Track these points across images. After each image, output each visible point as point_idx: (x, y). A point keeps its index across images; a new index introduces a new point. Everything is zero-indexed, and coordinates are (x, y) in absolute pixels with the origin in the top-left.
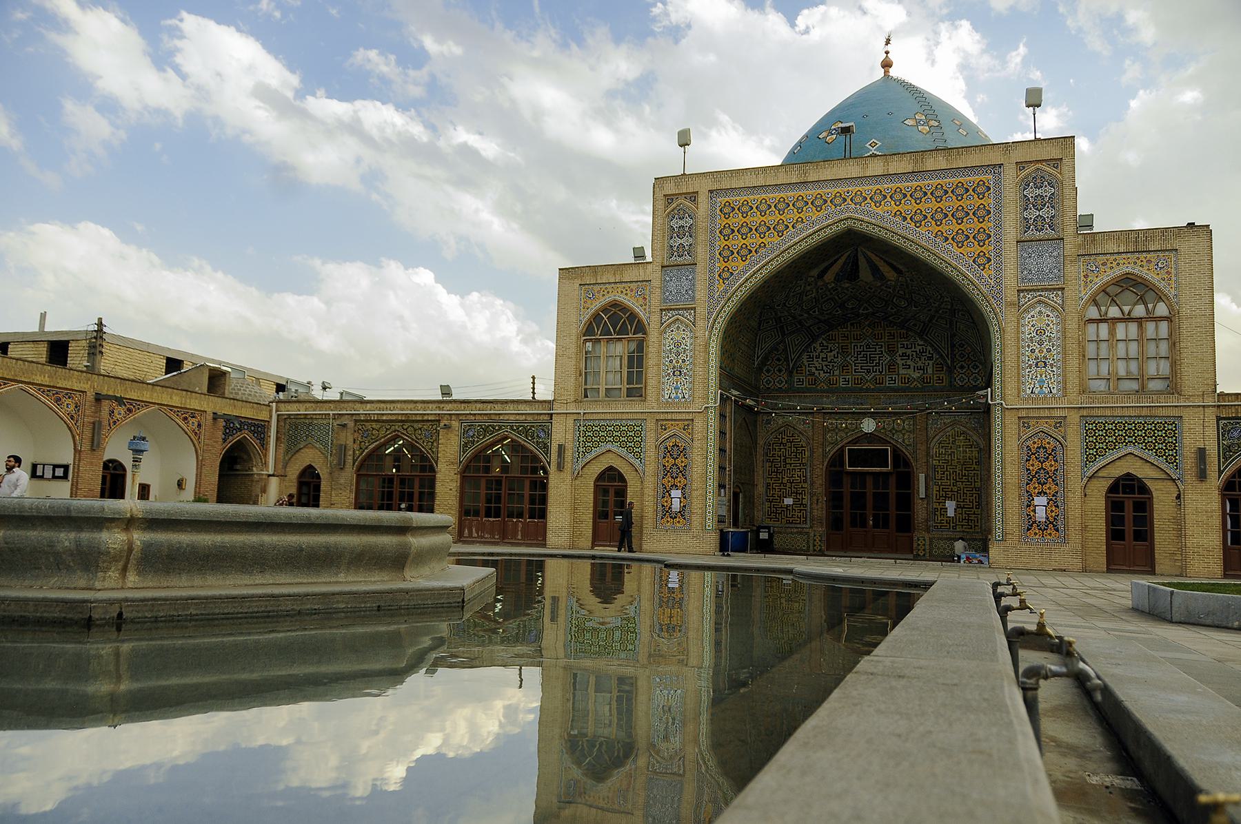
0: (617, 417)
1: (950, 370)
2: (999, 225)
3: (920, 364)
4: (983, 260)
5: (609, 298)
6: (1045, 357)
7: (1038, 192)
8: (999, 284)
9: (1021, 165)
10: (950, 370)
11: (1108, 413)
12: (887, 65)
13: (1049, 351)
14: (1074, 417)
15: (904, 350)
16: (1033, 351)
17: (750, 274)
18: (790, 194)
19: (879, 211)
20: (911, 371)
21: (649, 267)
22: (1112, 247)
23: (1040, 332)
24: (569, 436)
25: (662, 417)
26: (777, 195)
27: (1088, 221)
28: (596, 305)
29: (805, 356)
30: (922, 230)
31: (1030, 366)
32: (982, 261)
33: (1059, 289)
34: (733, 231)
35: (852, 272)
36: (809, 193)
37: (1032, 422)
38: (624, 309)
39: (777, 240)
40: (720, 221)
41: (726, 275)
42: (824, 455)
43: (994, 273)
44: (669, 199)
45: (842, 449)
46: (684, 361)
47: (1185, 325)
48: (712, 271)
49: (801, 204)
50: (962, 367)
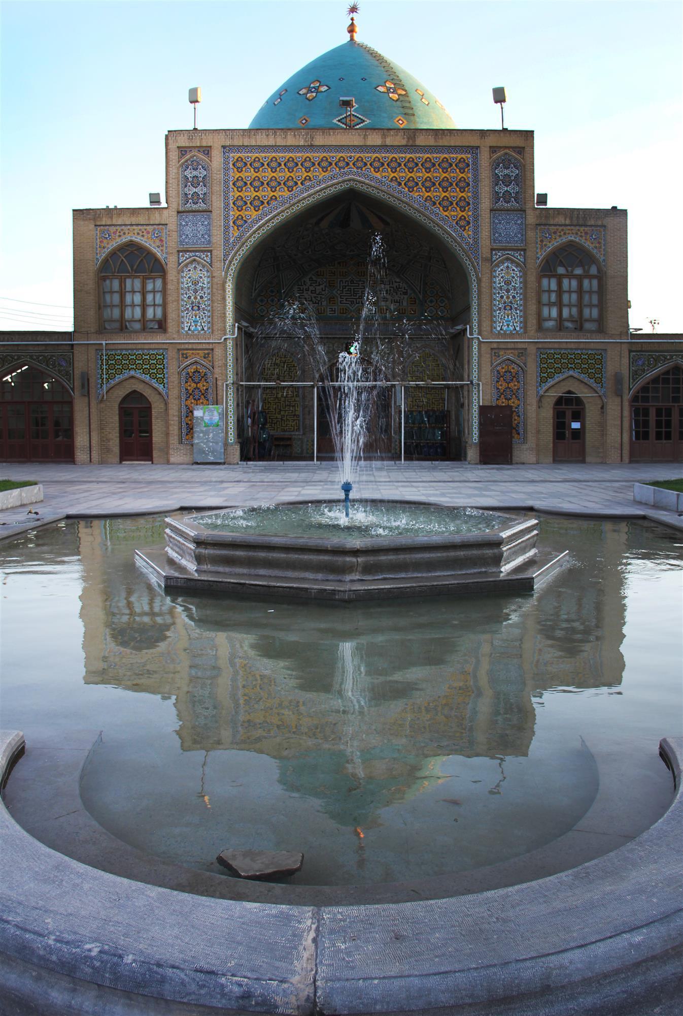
0: (139, 346)
2: (476, 196)
4: (463, 223)
6: (511, 302)
7: (506, 172)
9: (493, 149)
14: (532, 350)
16: (502, 297)
17: (262, 223)
18: (299, 155)
19: (378, 175)
21: (165, 212)
22: (561, 220)
25: (183, 347)
27: (543, 198)
31: (500, 309)
32: (462, 223)
33: (522, 250)
34: (246, 184)
36: (317, 156)
37: (501, 353)
39: (286, 194)
40: (234, 174)
41: (239, 222)
44: (183, 151)
46: (202, 297)
48: (226, 218)
49: (308, 164)
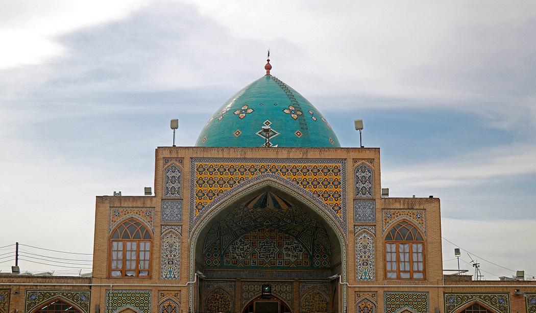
0: (134, 288)
1: (312, 258)
2: (344, 190)
3: (295, 254)
4: (337, 208)
5: (128, 216)
6: (367, 260)
7: (363, 174)
8: (345, 221)
9: (355, 160)
10: (312, 258)
11: (396, 290)
12: (268, 67)
13: (369, 257)
14: (381, 292)
15: (287, 246)
16: (361, 257)
17: (214, 208)
18: (237, 164)
19: (285, 177)
21: (154, 199)
22: (397, 206)
23: (365, 247)
24: (103, 300)
25: (162, 289)
26: (230, 164)
27: (386, 192)
28: (120, 220)
29: (231, 247)
30: (307, 190)
31: (360, 265)
32: (336, 208)
33: (373, 226)
34: (204, 182)
35: (263, 204)
36: (248, 164)
37: (361, 294)
38: (138, 223)
39: (229, 189)
40: (197, 176)
41: (200, 207)
42: (242, 305)
43: (343, 218)
44: (166, 160)
45: (252, 303)
46: (175, 256)
47: (429, 246)
48: (192, 204)
49: (242, 170)
50: (318, 256)
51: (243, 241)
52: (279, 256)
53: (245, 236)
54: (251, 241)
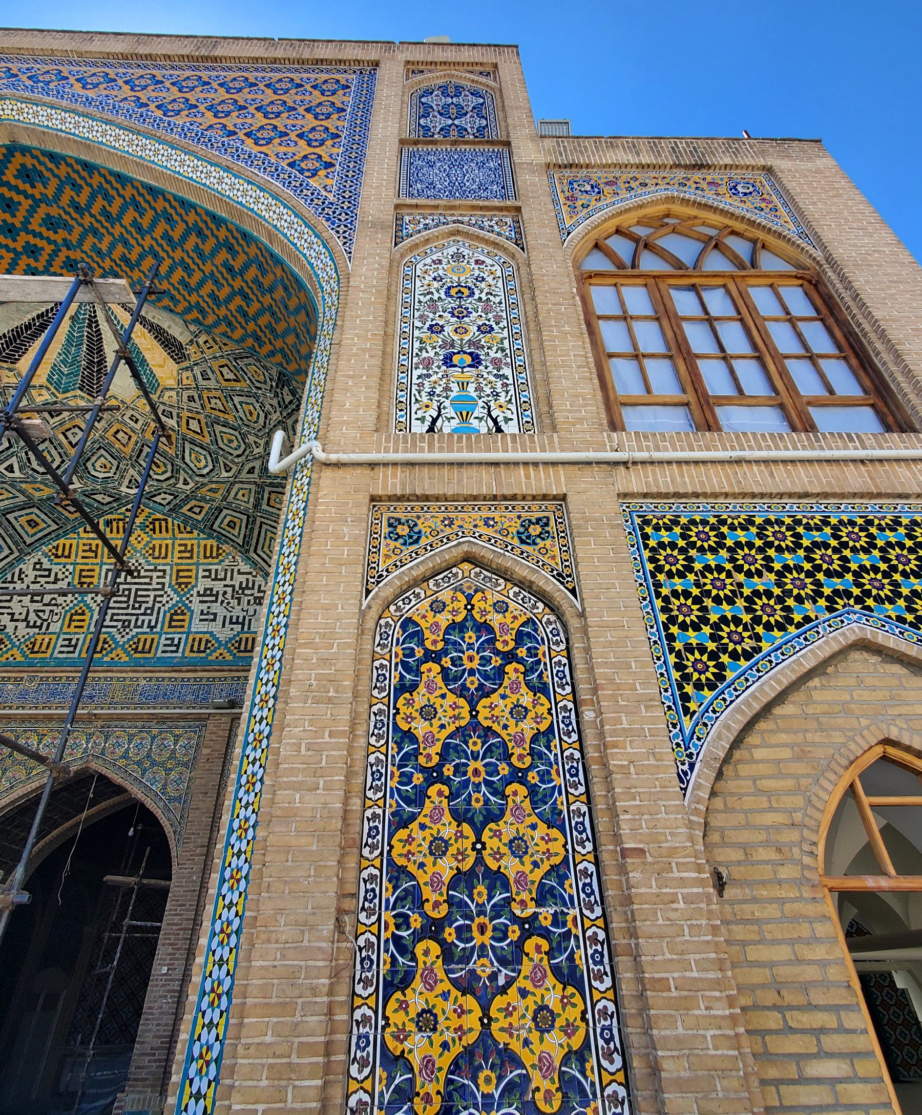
3: (237, 612)
15: (209, 583)
20: (215, 627)
51: (46, 565)
52: (171, 620)
53: (57, 548)
54: (75, 564)
